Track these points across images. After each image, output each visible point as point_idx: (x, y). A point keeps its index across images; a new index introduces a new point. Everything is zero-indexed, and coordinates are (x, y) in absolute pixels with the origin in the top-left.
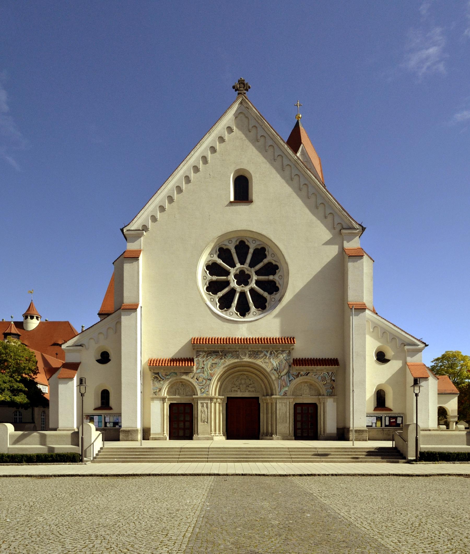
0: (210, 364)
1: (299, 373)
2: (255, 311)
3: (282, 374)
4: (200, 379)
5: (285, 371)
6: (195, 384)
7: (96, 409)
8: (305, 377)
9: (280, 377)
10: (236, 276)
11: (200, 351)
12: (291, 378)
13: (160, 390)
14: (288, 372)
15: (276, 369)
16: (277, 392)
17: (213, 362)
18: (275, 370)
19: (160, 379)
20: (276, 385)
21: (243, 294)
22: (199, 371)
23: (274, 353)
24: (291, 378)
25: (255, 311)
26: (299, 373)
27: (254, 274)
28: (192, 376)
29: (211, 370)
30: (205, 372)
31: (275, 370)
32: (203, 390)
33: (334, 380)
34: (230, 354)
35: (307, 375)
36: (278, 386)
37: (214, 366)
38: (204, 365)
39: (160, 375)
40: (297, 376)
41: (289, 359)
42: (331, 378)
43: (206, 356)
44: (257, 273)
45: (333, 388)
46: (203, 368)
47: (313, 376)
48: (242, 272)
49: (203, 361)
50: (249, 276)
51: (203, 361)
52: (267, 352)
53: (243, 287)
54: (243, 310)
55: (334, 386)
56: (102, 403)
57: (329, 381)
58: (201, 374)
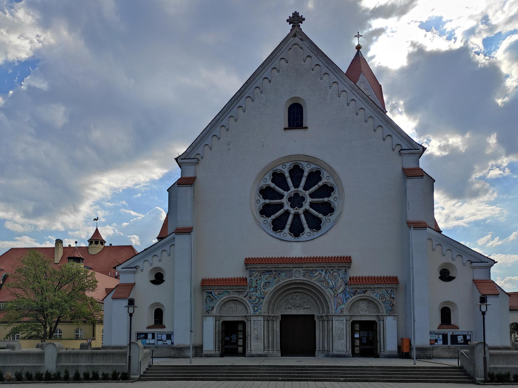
0: (263, 282)
1: (356, 291)
2: (309, 231)
3: (338, 293)
4: (253, 298)
5: (341, 289)
6: (247, 301)
7: (148, 328)
8: (362, 295)
9: (336, 295)
10: (290, 199)
11: (253, 271)
12: (348, 296)
13: (213, 308)
14: (344, 291)
15: (332, 287)
16: (333, 309)
17: (267, 281)
18: (330, 288)
19: (212, 298)
20: (332, 303)
21: (297, 216)
22: (252, 290)
23: (329, 272)
24: (348, 296)
25: (309, 231)
26: (356, 291)
27: (308, 196)
28: (245, 295)
29: (264, 289)
30: (258, 291)
31: (330, 288)
32: (256, 309)
33: (393, 298)
34: (284, 273)
35: (364, 293)
36: (334, 302)
37: (267, 285)
38: (257, 284)
39: (213, 294)
40: (354, 294)
41: (345, 278)
42: (390, 296)
43: (259, 275)
44: (311, 196)
45: (393, 305)
46: (256, 287)
47: (371, 294)
48: (296, 195)
49: (257, 281)
50: (303, 199)
51: (257, 281)
52: (322, 271)
53: (297, 209)
54: (297, 231)
55: (394, 303)
56: (156, 322)
57: (388, 299)
58: (254, 293)
